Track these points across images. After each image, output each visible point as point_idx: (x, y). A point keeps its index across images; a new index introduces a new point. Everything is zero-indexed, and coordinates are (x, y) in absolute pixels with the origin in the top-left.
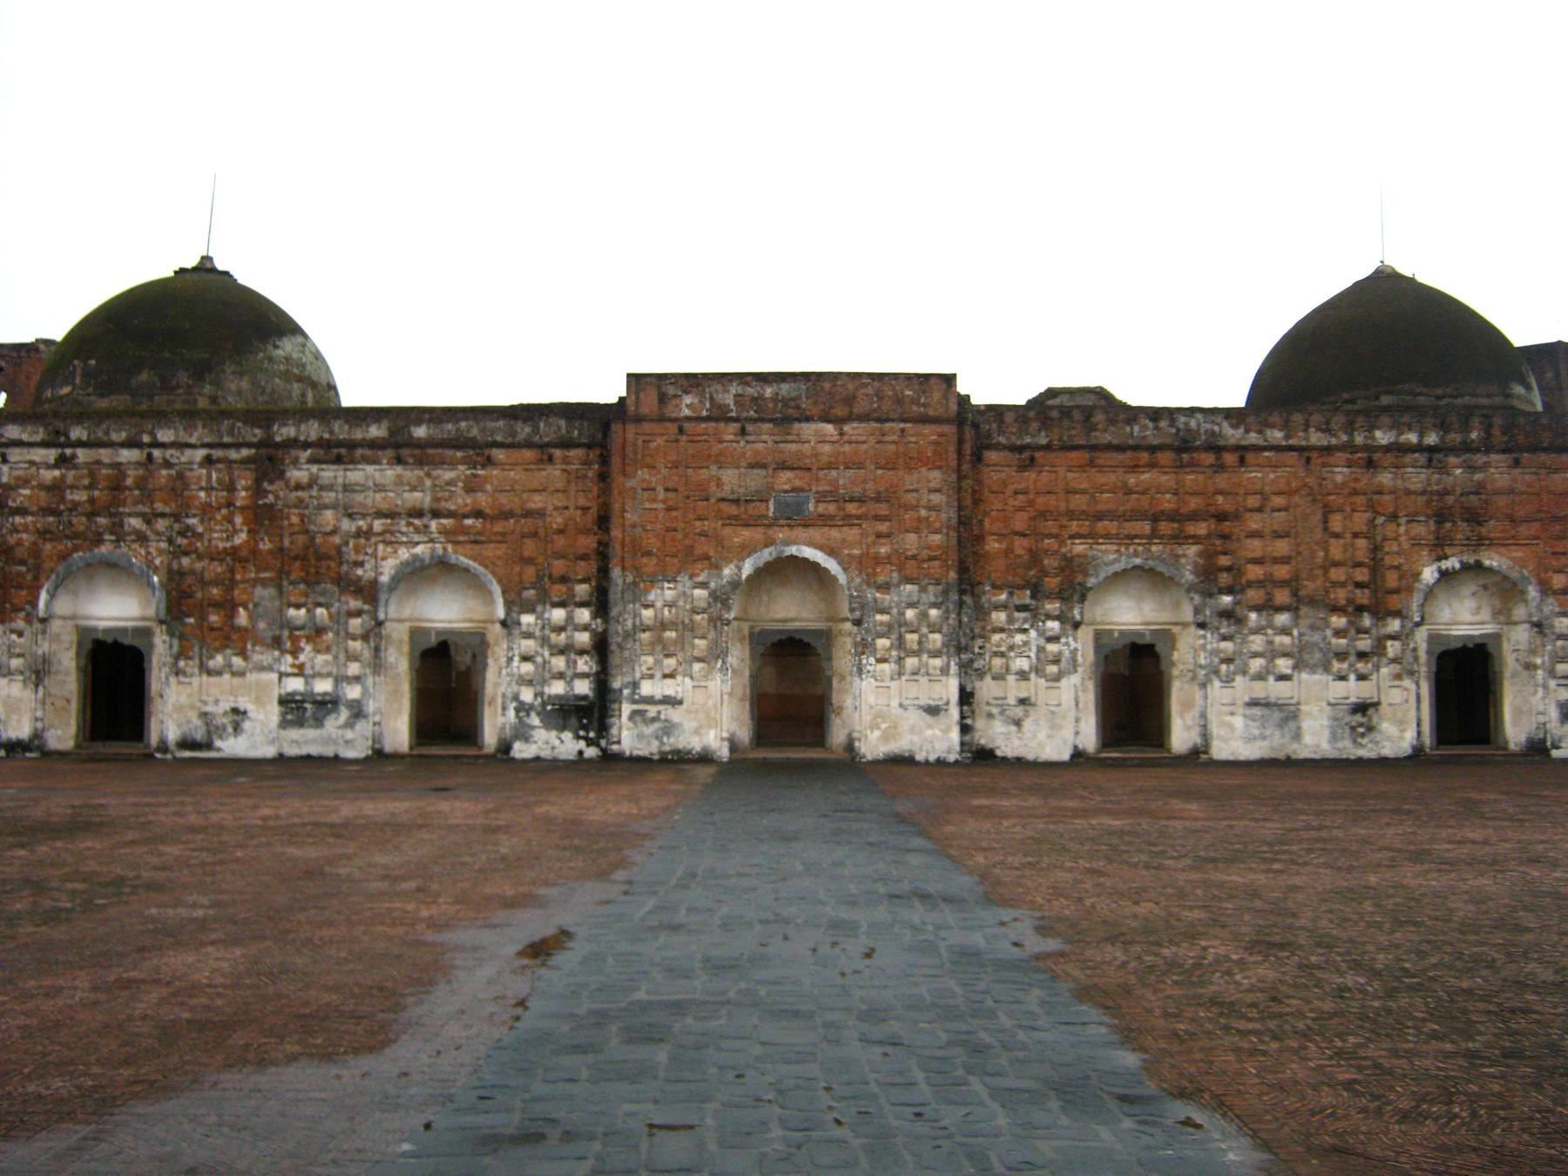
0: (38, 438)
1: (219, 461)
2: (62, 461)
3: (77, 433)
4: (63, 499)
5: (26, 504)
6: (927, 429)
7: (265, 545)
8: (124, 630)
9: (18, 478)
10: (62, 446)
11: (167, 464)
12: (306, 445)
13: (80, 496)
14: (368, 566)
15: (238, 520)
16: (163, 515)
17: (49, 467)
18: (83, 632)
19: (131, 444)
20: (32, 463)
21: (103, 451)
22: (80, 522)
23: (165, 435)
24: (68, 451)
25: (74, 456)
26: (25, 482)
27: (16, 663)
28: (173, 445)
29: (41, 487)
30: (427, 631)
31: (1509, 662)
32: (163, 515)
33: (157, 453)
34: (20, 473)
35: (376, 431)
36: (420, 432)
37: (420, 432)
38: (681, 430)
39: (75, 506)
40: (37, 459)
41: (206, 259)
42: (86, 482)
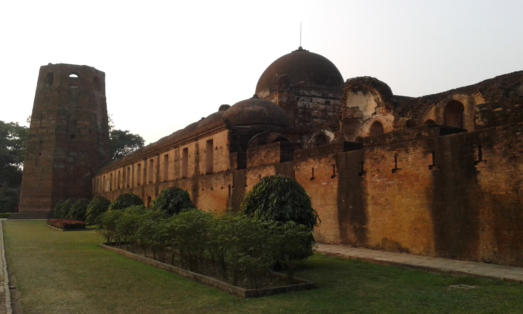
0: (320, 95)
2: (327, 103)
4: (326, 115)
5: (316, 115)
9: (314, 107)
13: (331, 114)
17: (323, 104)
20: (318, 103)
21: (337, 101)
25: (330, 102)
26: (316, 109)
29: (321, 110)
34: (315, 105)
39: (330, 117)
40: (320, 102)
41: (300, 49)
42: (332, 110)
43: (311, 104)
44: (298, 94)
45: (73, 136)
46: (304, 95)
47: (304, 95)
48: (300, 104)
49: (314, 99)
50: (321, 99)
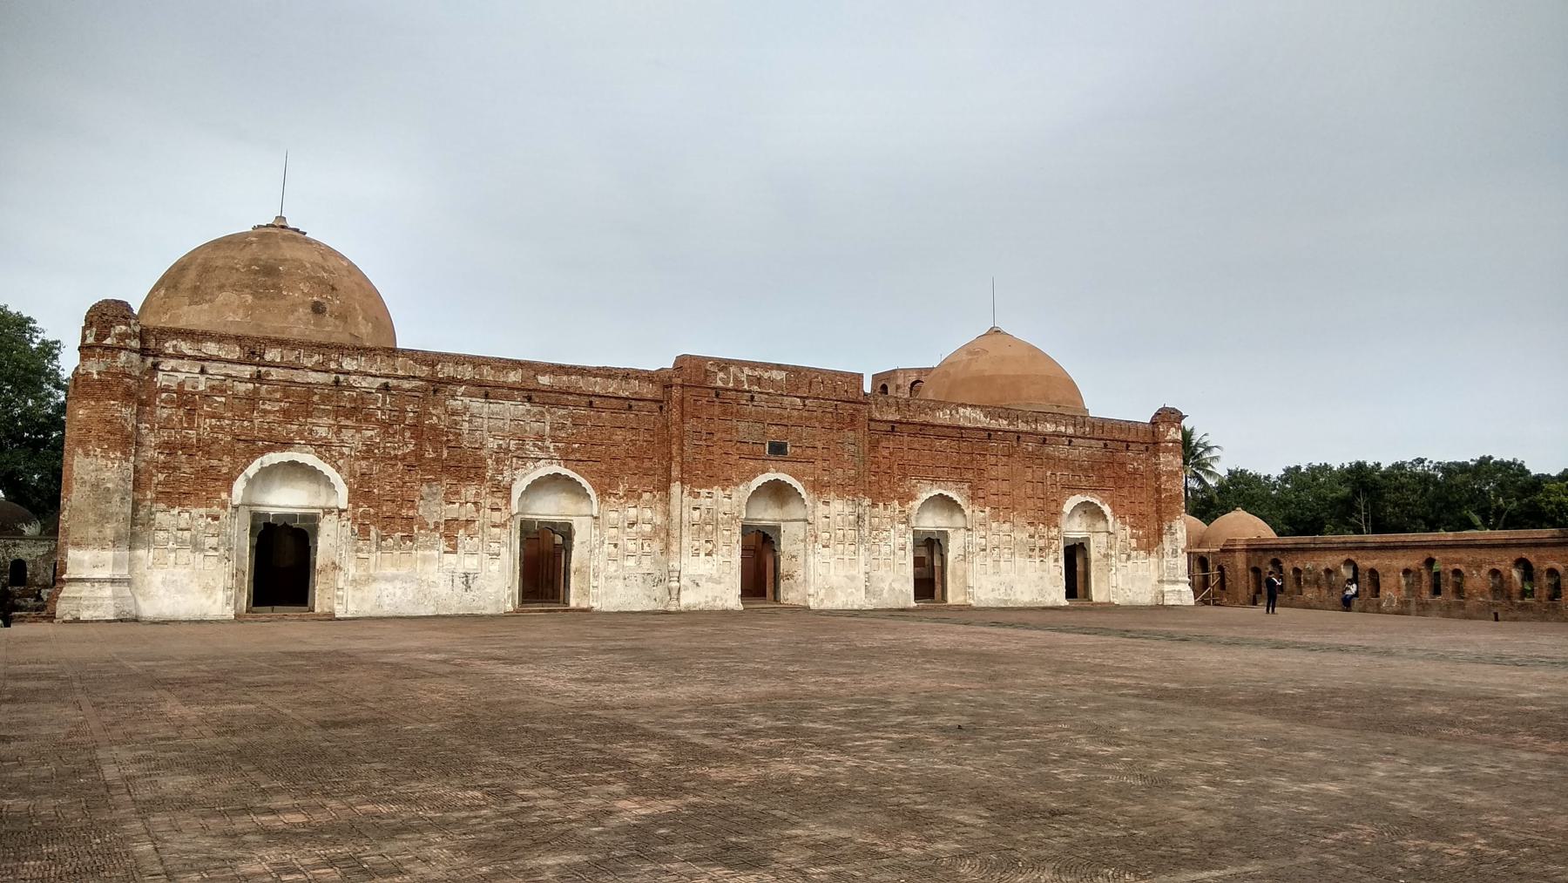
1: (396, 388)
2: (258, 378)
3: (272, 355)
6: (848, 406)
7: (430, 454)
8: (295, 515)
9: (212, 388)
10: (258, 365)
11: (351, 387)
12: (461, 382)
14: (506, 473)
15: (408, 434)
16: (346, 427)
18: (255, 516)
19: (321, 368)
20: (228, 376)
23: (349, 364)
24: (263, 370)
25: (269, 374)
27: (213, 541)
28: (356, 372)
30: (532, 522)
31: (1094, 554)
32: (346, 427)
33: (342, 378)
35: (514, 377)
36: (544, 380)
37: (544, 380)
38: (717, 395)
40: (234, 374)
43: (202, 378)
46: (182, 356)
47: (182, 356)
48: (161, 379)
49: (212, 368)
50: (239, 367)
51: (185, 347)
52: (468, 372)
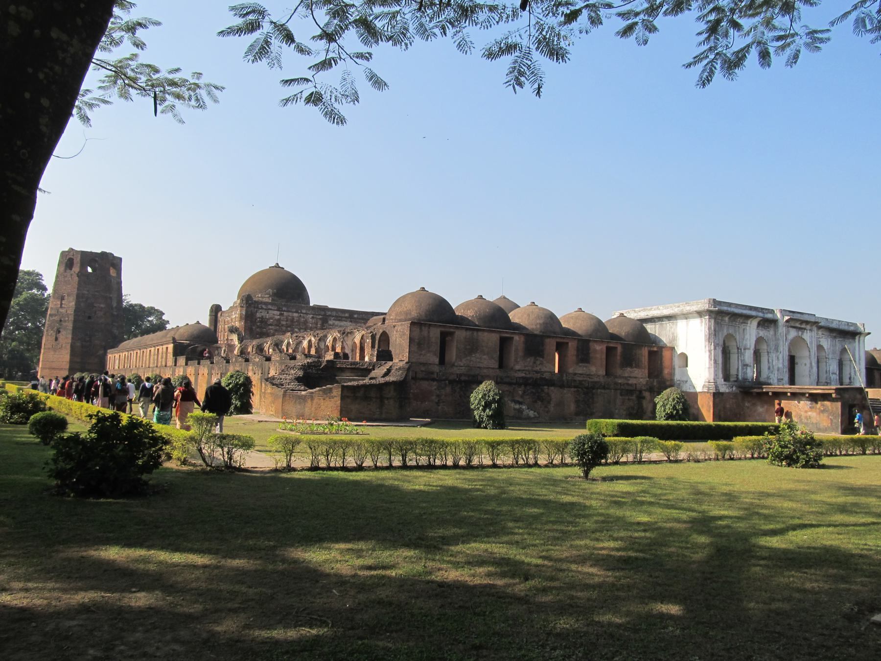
13: (284, 323)
19: (296, 312)
22: (284, 328)
23: (304, 311)
35: (347, 315)
36: (356, 316)
44: (257, 307)
45: (90, 318)
46: (262, 308)
47: (262, 308)
48: (258, 315)
51: (264, 307)
52: (334, 313)
